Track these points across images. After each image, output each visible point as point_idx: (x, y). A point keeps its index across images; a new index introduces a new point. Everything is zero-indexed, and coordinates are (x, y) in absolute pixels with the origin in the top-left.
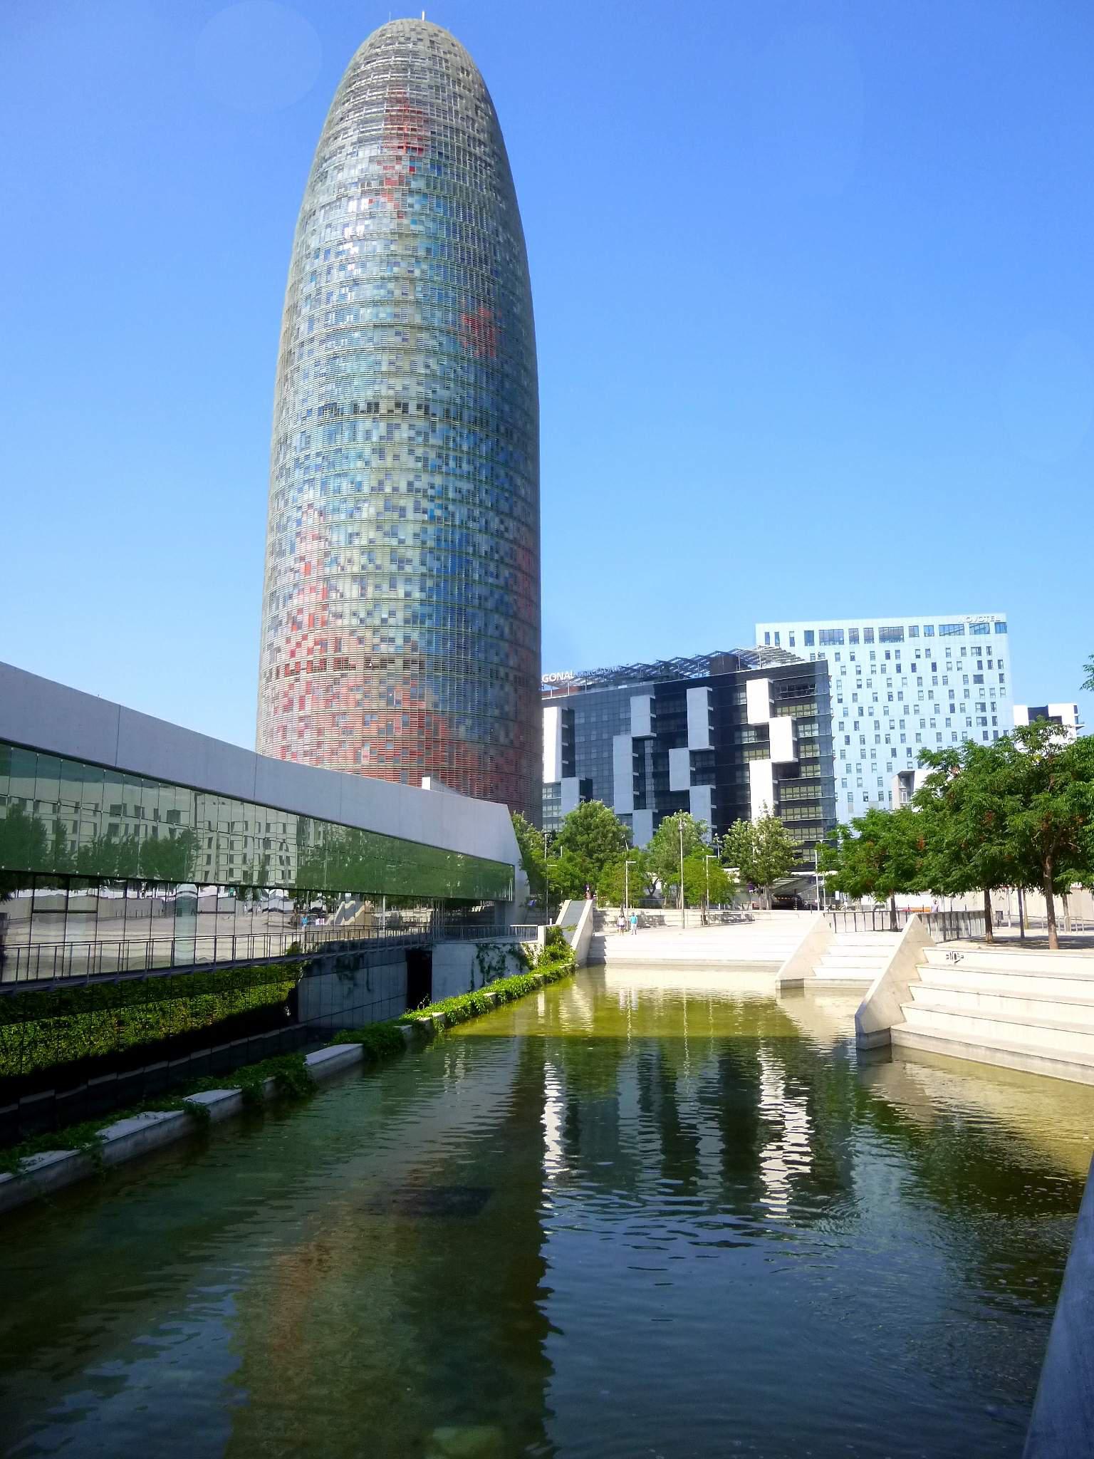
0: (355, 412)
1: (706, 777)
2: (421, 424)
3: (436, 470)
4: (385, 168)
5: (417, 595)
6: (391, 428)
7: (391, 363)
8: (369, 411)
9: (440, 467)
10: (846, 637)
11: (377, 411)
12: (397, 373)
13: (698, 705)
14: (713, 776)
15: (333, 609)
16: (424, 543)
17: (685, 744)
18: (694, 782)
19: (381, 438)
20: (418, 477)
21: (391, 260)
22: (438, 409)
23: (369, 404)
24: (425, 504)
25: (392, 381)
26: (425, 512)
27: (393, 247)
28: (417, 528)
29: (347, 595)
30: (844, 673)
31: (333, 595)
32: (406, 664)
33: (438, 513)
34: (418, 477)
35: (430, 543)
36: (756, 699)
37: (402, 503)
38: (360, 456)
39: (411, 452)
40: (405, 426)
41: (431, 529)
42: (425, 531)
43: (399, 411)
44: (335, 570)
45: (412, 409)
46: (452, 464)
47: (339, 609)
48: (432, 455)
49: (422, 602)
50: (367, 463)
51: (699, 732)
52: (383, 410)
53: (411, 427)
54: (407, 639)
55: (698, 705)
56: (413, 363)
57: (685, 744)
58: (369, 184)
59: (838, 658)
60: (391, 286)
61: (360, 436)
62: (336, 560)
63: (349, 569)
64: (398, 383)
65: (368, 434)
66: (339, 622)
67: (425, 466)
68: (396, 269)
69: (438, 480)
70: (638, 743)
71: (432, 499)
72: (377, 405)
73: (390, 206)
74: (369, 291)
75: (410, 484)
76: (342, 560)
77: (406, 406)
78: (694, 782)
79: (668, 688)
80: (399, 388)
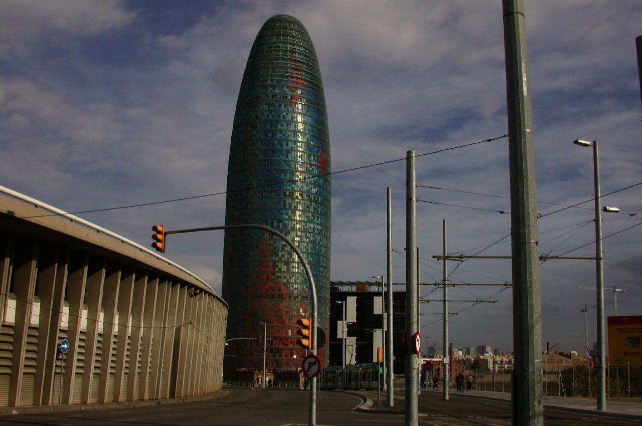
0: (284, 195)
3: (312, 222)
4: (293, 92)
8: (290, 196)
11: (293, 196)
13: (352, 302)
15: (277, 275)
16: (308, 250)
20: (306, 225)
22: (312, 197)
23: (290, 193)
26: (308, 237)
29: (283, 270)
31: (277, 269)
32: (303, 298)
38: (287, 214)
44: (277, 259)
47: (280, 275)
50: (290, 217)
54: (303, 288)
58: (286, 97)
61: (287, 207)
62: (278, 256)
63: (283, 259)
65: (290, 204)
66: (279, 280)
69: (312, 226)
71: (310, 233)
72: (293, 193)
76: (280, 256)
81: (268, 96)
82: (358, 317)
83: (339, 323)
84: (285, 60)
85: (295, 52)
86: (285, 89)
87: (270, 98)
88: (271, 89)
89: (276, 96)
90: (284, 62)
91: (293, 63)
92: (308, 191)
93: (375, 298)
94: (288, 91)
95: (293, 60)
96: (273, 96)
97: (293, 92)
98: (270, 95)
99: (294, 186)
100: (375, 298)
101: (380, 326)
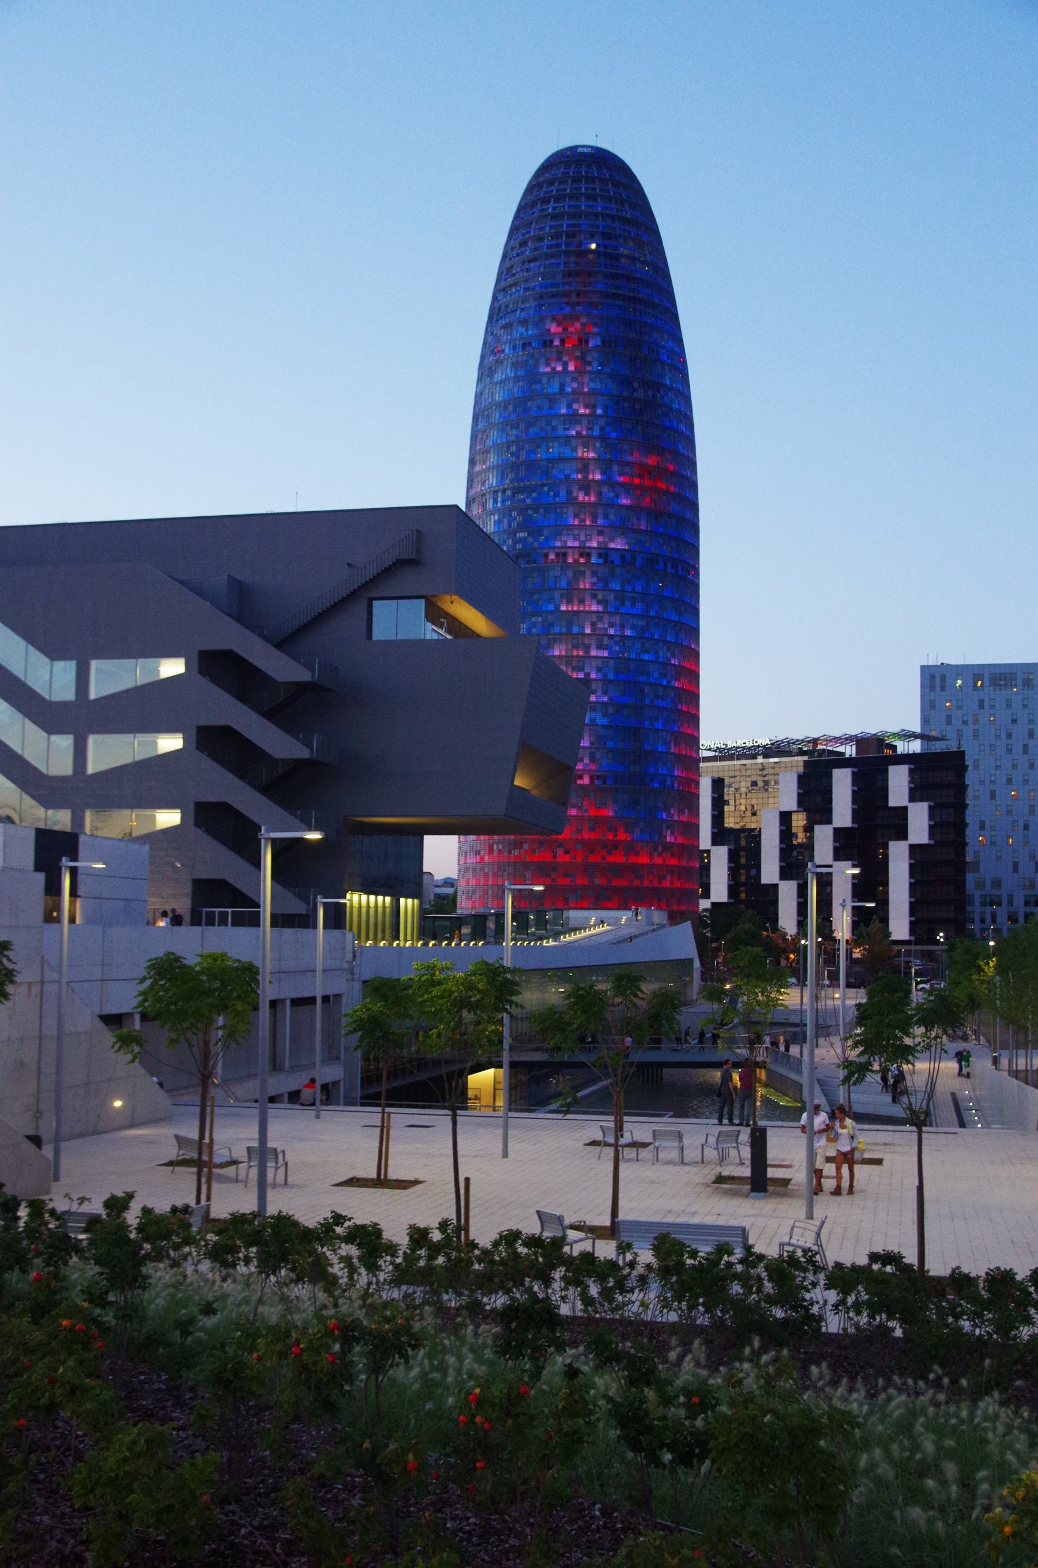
9: (617, 608)
10: (1019, 681)
13: (842, 782)
17: (829, 821)
28: (600, 664)
30: (1014, 721)
36: (898, 783)
37: (587, 641)
40: (588, 573)
46: (628, 604)
48: (611, 597)
49: (604, 727)
53: (594, 574)
55: (842, 782)
57: (829, 821)
58: (551, 342)
59: (1009, 705)
67: (605, 608)
70: (785, 818)
79: (817, 766)
93: (891, 768)
94: (554, 328)
100: (891, 768)
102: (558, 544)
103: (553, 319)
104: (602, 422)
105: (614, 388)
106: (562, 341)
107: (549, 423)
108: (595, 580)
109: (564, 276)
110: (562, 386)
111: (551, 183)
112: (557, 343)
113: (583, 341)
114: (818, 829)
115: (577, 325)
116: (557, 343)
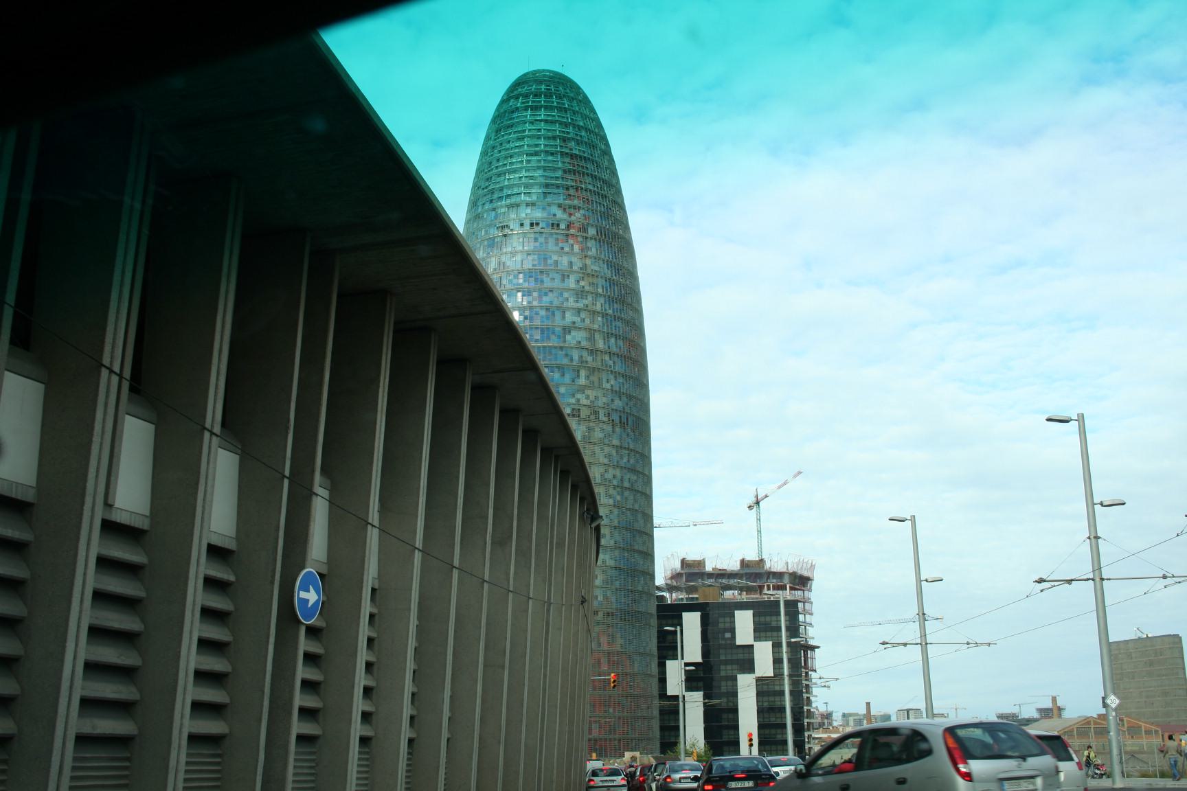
1: (694, 684)
2: (609, 428)
4: (570, 215)
5: (611, 563)
6: (590, 429)
7: (587, 377)
12: (591, 386)
14: (701, 684)
18: (689, 688)
19: (584, 437)
20: (606, 471)
21: (580, 294)
22: (616, 417)
24: (611, 491)
25: (588, 392)
26: (610, 496)
27: (582, 283)
33: (618, 498)
34: (606, 471)
35: (616, 523)
39: (602, 450)
41: (616, 511)
42: (611, 512)
43: (593, 417)
45: (602, 417)
48: (614, 452)
51: (692, 649)
52: (583, 415)
53: (602, 430)
54: (606, 598)
56: (600, 380)
60: (583, 315)
64: (591, 393)
68: (586, 302)
71: (615, 487)
73: (576, 248)
74: (570, 317)
75: (602, 475)
77: (596, 413)
78: (689, 688)
80: (592, 398)
81: (522, 225)
82: (705, 653)
83: (698, 658)
84: (552, 154)
85: (570, 139)
86: (554, 209)
87: (527, 227)
88: (529, 210)
89: (538, 224)
90: (550, 158)
91: (567, 160)
92: (606, 406)
93: (737, 613)
94: (560, 214)
95: (567, 154)
96: (532, 225)
97: (570, 215)
98: (527, 223)
99: (579, 396)
100: (737, 613)
101: (749, 666)
102: (573, 401)
103: (560, 206)
104: (602, 300)
105: (608, 273)
106: (568, 227)
107: (561, 294)
108: (601, 435)
109: (565, 172)
110: (571, 263)
111: (526, 96)
112: (563, 226)
113: (583, 229)
114: (669, 663)
115: (578, 215)
116: (563, 226)
